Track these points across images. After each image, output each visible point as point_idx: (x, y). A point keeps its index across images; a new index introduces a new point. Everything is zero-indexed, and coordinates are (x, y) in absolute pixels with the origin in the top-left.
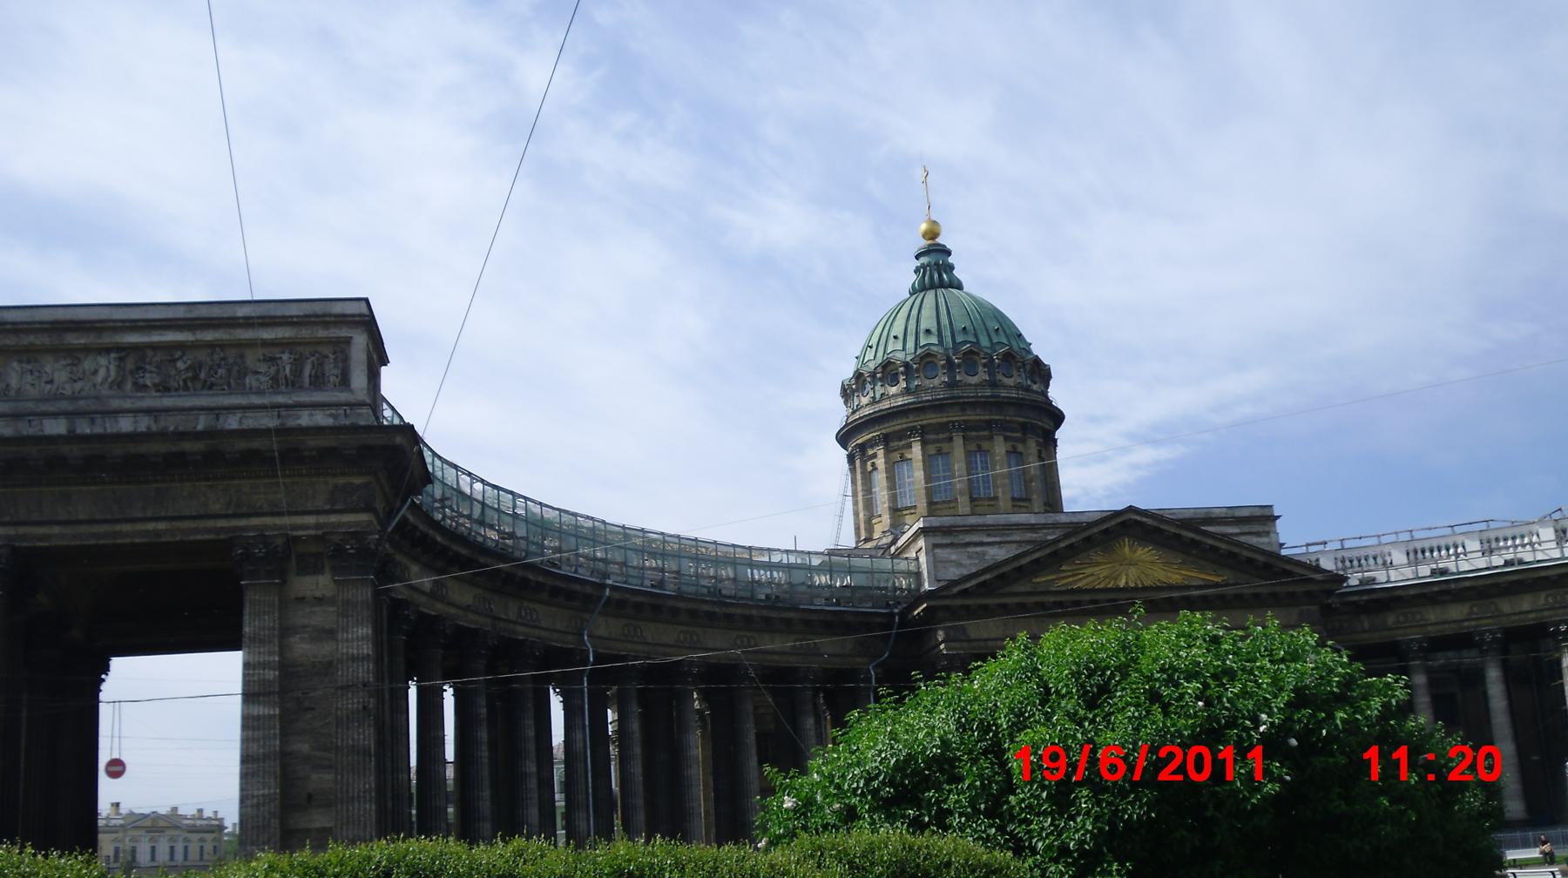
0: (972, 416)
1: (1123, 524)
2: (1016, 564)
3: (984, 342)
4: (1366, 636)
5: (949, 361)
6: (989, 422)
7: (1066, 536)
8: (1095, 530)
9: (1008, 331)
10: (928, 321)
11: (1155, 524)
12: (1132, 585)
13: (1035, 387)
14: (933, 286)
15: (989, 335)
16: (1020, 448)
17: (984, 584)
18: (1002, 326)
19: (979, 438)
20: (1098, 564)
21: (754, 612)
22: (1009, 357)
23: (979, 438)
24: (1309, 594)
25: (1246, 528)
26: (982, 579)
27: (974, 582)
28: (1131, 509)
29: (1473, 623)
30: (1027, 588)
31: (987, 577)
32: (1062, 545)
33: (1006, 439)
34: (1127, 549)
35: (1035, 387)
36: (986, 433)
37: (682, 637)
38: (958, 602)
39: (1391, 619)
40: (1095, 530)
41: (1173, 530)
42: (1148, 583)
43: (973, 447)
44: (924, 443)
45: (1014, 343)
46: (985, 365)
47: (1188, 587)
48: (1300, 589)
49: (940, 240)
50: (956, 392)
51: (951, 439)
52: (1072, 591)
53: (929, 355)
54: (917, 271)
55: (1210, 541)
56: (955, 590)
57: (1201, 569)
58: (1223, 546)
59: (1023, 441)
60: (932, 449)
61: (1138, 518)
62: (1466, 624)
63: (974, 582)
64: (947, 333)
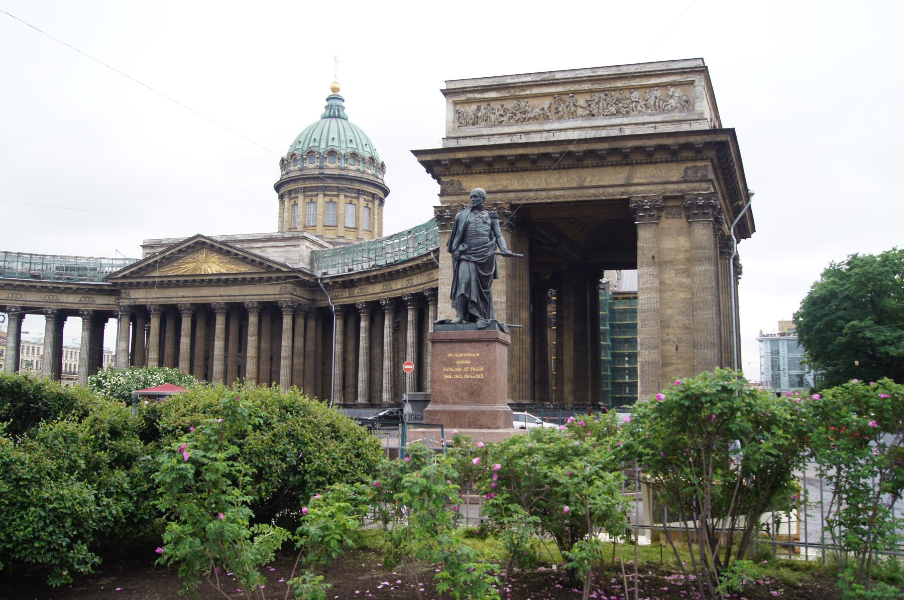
0: (308, 184)
1: (197, 243)
2: (147, 263)
3: (323, 145)
4: (346, 300)
5: (302, 156)
6: (316, 187)
7: (168, 250)
8: (183, 246)
9: (343, 138)
10: (302, 139)
11: (211, 242)
12: (203, 273)
13: (352, 168)
14: (329, 117)
15: (327, 142)
16: (335, 199)
17: (132, 273)
18: (339, 136)
19: (311, 195)
20: (191, 262)
21: (48, 285)
22: (332, 153)
23: (311, 195)
24: (278, 278)
25: (288, 243)
26: (132, 270)
27: (128, 271)
28: (199, 236)
29: (382, 294)
30: (157, 275)
31: (134, 269)
32: (167, 253)
33: (325, 195)
34: (204, 255)
35: (352, 168)
36: (316, 193)
37: (10, 295)
38: (120, 281)
39: (356, 291)
40: (183, 246)
41: (218, 245)
42: (210, 273)
43: (308, 200)
44: (291, 199)
45: (343, 145)
46: (318, 158)
47: (229, 274)
48: (274, 275)
49: (339, 93)
50: (304, 172)
51: (298, 197)
52: (177, 276)
53: (294, 154)
54: (326, 107)
55: (235, 251)
56: (120, 275)
57: (238, 265)
58: (240, 253)
59: (338, 196)
60: (292, 201)
61: (204, 240)
62: (380, 295)
63: (128, 271)
64: (307, 142)
